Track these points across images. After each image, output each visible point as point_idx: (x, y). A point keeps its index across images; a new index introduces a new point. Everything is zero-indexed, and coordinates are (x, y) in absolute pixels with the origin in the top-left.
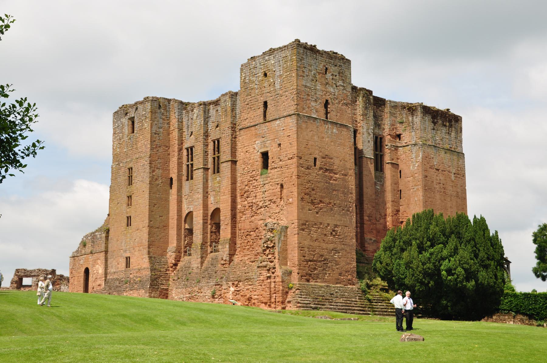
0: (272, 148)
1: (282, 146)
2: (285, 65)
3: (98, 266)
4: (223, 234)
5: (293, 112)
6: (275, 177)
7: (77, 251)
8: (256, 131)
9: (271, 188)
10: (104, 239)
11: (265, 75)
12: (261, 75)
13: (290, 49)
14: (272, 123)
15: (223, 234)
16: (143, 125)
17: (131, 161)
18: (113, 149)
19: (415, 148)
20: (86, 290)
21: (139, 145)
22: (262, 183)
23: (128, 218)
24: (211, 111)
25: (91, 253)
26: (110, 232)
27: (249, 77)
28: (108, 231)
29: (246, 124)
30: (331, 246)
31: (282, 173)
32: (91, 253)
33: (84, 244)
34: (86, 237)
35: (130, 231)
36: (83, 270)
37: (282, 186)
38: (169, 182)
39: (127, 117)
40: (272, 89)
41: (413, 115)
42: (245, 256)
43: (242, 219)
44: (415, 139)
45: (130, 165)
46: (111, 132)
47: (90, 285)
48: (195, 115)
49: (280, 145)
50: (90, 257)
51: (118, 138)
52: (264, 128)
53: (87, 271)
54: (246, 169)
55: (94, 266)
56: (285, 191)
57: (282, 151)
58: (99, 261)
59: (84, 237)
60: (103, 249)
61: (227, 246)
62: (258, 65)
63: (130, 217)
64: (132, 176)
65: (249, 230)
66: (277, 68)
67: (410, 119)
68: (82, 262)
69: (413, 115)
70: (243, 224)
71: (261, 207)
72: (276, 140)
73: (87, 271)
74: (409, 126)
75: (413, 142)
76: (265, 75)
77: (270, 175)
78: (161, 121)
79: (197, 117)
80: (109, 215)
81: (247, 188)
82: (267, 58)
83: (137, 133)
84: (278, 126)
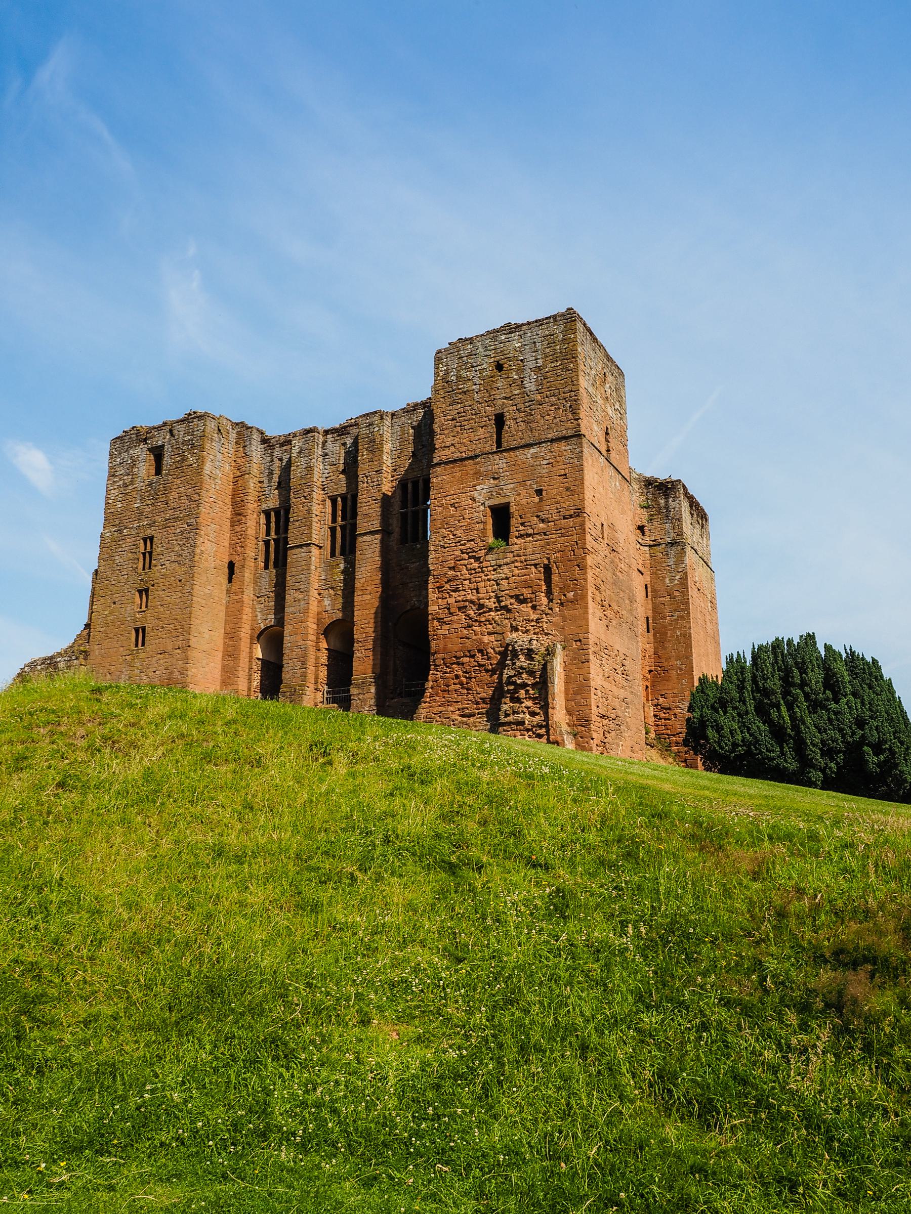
0: (519, 498)
1: (544, 493)
2: (548, 350)
4: (361, 667)
5: (570, 433)
6: (529, 551)
8: (478, 466)
9: (516, 572)
11: (499, 367)
12: (487, 366)
13: (561, 322)
14: (518, 452)
15: (361, 667)
16: (184, 459)
17: (150, 525)
18: (107, 503)
19: (674, 549)
21: (173, 495)
22: (493, 563)
23: (137, 630)
24: (329, 444)
27: (458, 371)
29: (447, 454)
30: (622, 693)
31: (548, 544)
35: (142, 656)
37: (548, 570)
38: (227, 570)
40: (516, 392)
41: (667, 496)
42: (449, 703)
43: (439, 632)
44: (672, 534)
45: (149, 532)
48: (295, 451)
49: (539, 492)
51: (121, 482)
52: (500, 463)
54: (451, 537)
56: (555, 578)
57: (544, 503)
59: (26, 666)
61: (373, 690)
62: (481, 349)
63: (144, 629)
64: (150, 553)
65: (458, 654)
66: (529, 356)
67: (662, 502)
69: (667, 496)
70: (441, 641)
71: (490, 610)
72: (528, 483)
74: (659, 513)
75: (669, 540)
76: (499, 367)
77: (516, 548)
78: (219, 456)
79: (300, 453)
80: (87, 626)
81: (451, 573)
82: (503, 337)
83: (167, 475)
84: (534, 457)
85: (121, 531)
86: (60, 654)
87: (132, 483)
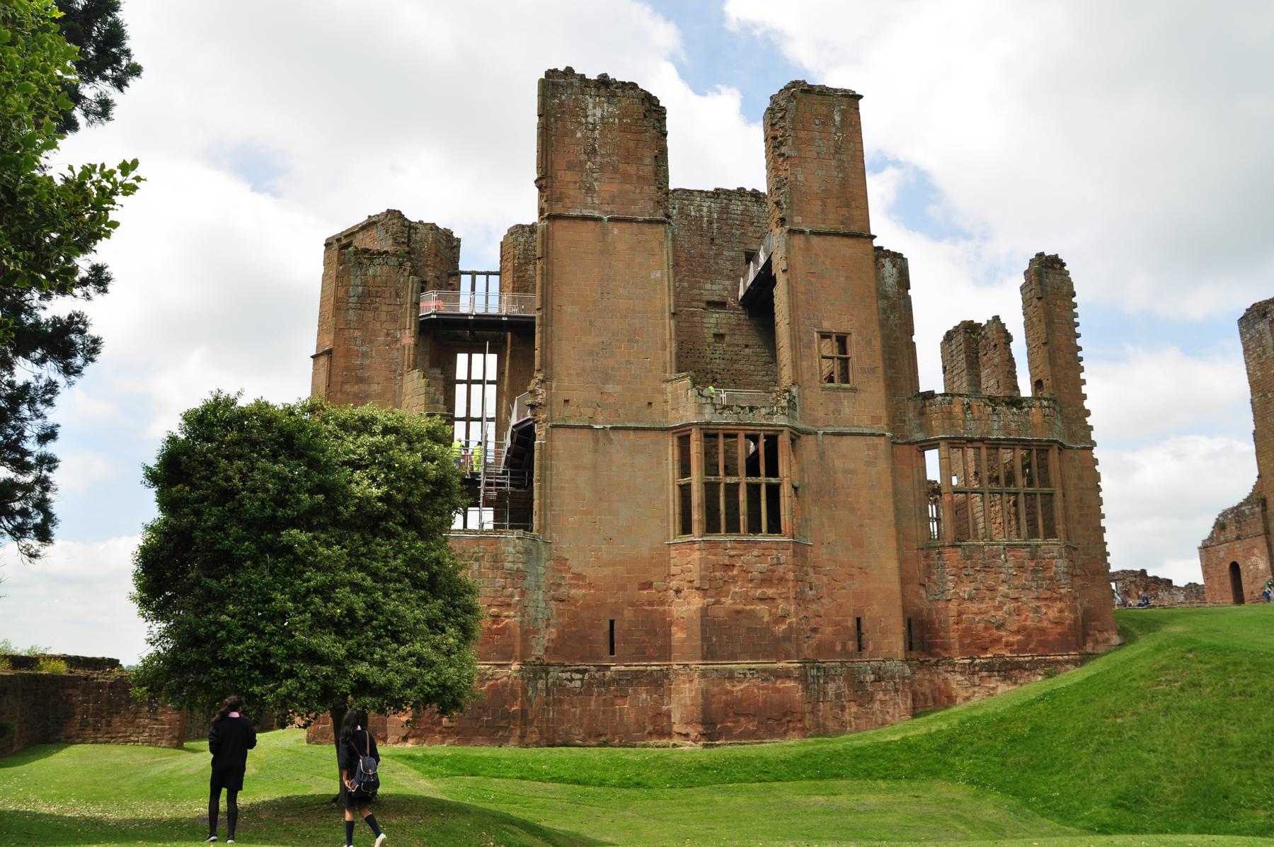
3: (1254, 558)
7: (1211, 538)
10: (1259, 515)
20: (1239, 598)
25: (1238, 538)
26: (1269, 503)
28: (1264, 502)
32: (1238, 538)
33: (1220, 526)
34: (1224, 514)
36: (1228, 566)
39: (1266, 321)
46: (1241, 348)
47: (1246, 588)
50: (1237, 545)
53: (1235, 568)
55: (1247, 558)
58: (1256, 551)
60: (1260, 530)
68: (1222, 554)
73: (1235, 568)
85: (1265, 395)
86: (1241, 505)
87: (1264, 352)
